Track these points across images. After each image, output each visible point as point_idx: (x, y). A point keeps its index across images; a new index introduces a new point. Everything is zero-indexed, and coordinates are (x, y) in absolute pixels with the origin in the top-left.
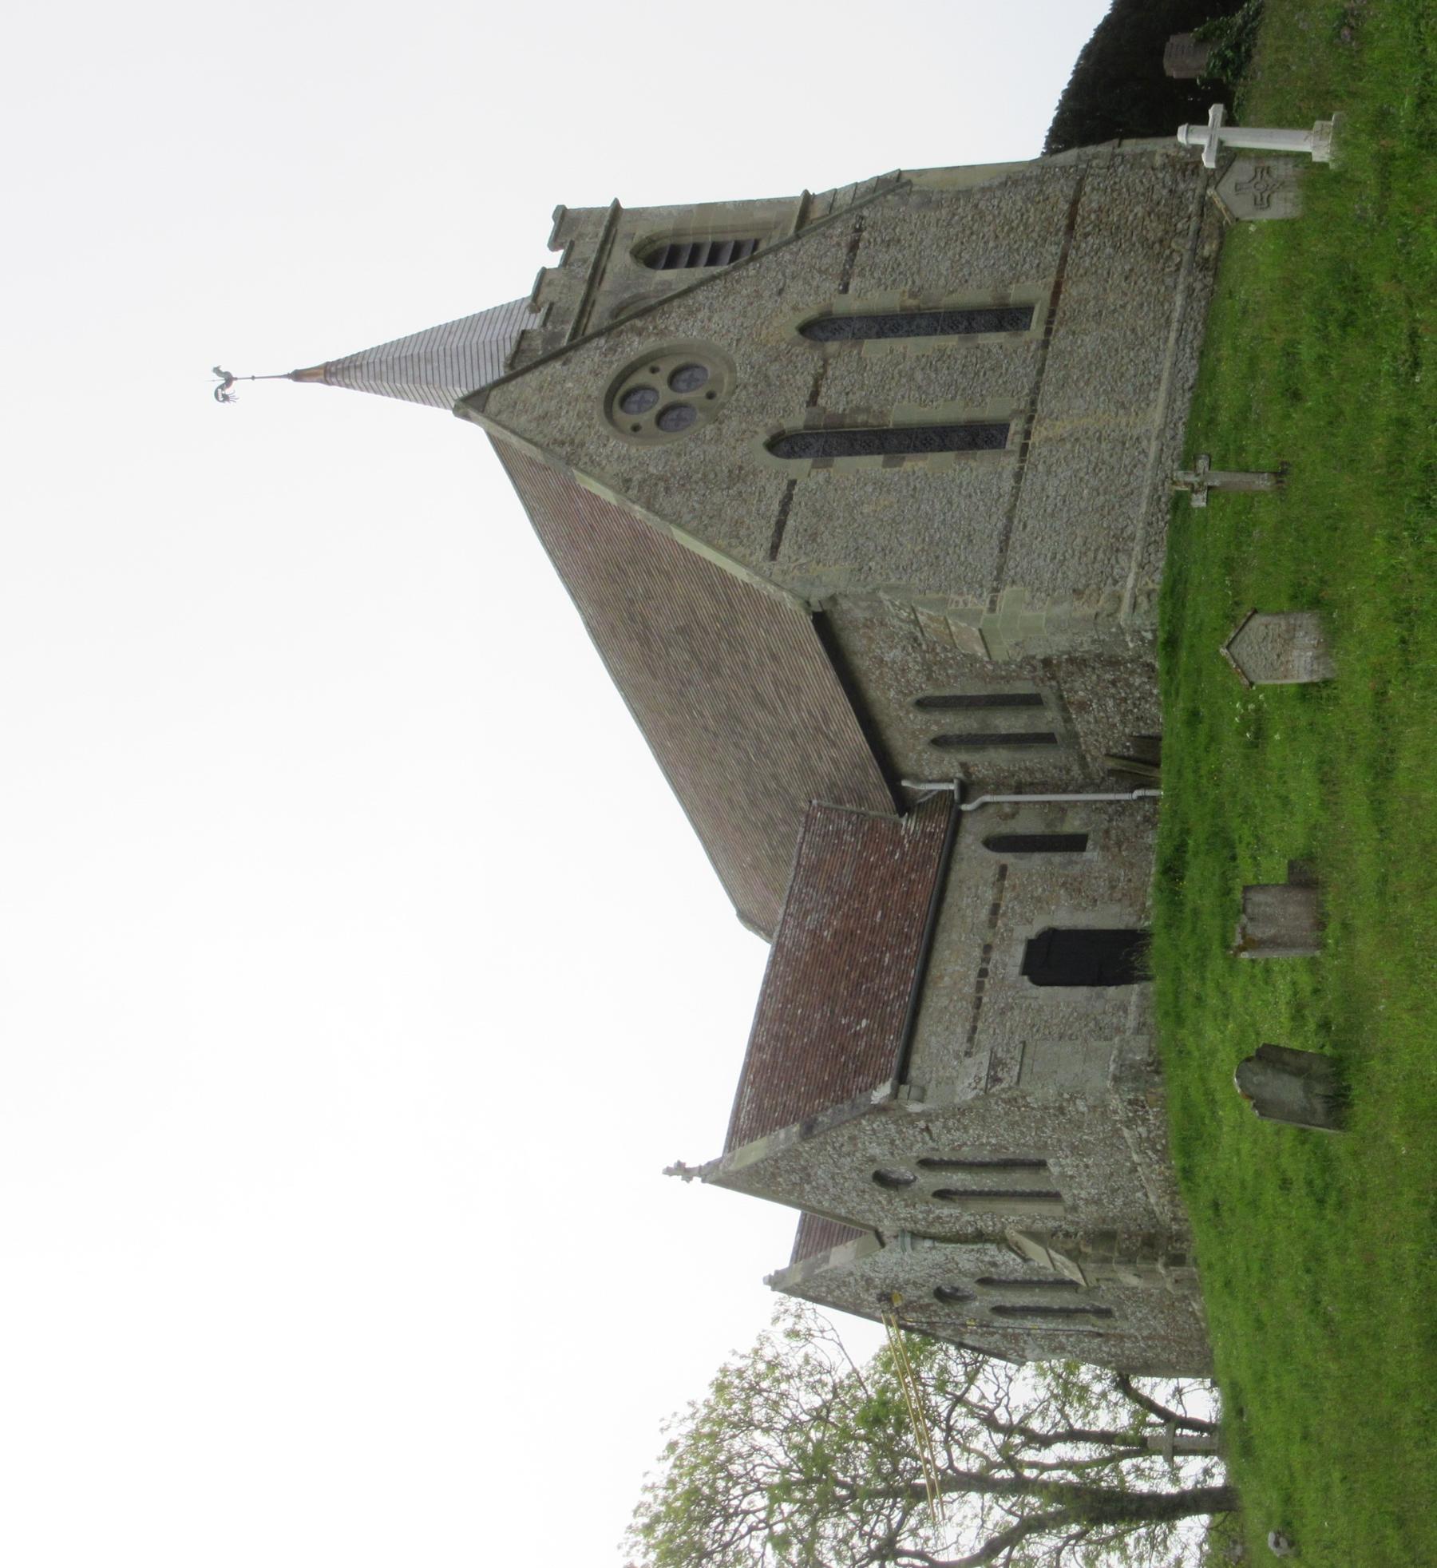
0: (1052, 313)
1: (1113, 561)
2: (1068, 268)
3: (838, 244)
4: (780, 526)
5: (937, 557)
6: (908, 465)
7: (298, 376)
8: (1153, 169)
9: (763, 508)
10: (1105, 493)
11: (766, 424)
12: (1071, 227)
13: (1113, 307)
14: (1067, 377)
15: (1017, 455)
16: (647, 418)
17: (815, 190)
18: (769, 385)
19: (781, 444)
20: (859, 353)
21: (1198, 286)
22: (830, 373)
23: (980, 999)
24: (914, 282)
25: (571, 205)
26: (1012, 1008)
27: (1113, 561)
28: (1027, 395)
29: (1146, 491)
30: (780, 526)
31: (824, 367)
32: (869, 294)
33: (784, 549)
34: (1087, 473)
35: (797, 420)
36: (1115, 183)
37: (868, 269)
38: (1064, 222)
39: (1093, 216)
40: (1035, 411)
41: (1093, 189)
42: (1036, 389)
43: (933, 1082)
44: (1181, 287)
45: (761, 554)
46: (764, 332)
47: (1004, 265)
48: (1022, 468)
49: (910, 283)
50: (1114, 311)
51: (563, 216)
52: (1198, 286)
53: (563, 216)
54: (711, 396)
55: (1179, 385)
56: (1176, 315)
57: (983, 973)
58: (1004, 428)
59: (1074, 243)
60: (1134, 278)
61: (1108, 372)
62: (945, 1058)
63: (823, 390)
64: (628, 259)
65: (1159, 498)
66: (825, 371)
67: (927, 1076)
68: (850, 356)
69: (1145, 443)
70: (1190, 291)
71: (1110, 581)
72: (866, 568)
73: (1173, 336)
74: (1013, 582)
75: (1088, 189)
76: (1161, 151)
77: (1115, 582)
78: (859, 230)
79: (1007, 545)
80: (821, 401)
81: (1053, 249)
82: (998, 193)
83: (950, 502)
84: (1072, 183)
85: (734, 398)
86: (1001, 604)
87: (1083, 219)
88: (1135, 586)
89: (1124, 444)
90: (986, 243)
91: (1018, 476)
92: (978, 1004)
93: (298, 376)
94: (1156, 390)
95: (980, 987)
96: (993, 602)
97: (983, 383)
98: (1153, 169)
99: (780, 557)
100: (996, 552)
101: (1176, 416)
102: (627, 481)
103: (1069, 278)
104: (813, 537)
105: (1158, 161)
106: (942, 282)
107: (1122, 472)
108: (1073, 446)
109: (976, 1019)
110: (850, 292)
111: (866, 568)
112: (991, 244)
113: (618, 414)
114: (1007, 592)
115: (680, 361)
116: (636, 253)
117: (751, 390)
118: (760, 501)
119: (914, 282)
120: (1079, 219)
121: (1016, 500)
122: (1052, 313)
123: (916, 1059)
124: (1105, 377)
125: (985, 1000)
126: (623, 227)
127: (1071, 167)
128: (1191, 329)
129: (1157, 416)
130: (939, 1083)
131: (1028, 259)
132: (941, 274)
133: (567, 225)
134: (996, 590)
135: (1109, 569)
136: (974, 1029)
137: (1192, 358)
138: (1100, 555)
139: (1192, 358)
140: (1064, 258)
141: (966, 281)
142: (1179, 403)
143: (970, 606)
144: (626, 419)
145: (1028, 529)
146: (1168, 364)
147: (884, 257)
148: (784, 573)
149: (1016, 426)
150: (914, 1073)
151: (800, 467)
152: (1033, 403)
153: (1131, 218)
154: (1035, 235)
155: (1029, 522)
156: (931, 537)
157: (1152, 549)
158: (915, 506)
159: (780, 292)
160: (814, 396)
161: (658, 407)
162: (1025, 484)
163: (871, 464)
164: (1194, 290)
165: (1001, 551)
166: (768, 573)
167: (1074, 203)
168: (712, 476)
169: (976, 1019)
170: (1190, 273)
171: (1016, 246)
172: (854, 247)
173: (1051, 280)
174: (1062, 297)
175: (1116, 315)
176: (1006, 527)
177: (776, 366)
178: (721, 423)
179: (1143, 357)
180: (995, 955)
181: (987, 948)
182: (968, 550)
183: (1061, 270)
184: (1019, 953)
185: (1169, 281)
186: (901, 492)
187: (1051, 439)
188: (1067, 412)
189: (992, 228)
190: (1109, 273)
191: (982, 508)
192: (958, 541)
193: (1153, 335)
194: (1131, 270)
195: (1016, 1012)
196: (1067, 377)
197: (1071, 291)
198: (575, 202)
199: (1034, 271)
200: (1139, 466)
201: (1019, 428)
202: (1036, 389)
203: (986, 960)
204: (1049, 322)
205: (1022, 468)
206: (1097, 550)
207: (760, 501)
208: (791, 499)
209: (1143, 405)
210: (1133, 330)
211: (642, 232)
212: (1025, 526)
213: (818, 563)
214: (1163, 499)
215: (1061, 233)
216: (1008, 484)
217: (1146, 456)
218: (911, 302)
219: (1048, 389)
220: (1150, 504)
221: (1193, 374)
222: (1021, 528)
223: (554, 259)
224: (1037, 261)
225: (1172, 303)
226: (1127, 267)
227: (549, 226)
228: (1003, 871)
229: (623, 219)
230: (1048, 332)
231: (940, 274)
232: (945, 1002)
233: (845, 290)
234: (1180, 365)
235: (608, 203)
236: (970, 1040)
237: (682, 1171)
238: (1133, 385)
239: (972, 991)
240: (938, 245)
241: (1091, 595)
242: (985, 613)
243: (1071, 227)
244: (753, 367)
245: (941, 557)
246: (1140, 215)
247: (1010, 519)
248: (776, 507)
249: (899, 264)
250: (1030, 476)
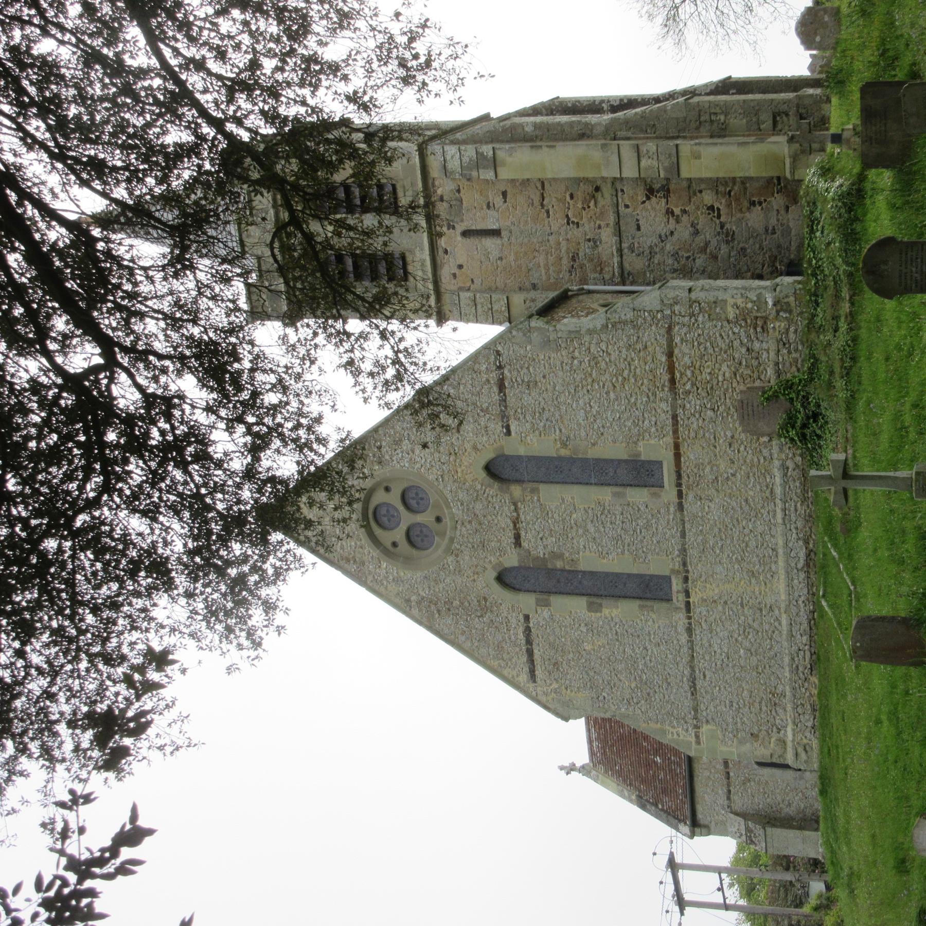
0: (679, 476)
1: (773, 712)
2: (681, 429)
3: (488, 381)
4: (530, 653)
5: (649, 694)
6: (606, 612)
8: (728, 321)
9: (513, 637)
10: (757, 654)
11: (490, 561)
12: (673, 381)
13: (726, 476)
14: (705, 542)
15: (684, 611)
16: (398, 534)
18: (480, 524)
20: (539, 500)
21: (790, 464)
22: (522, 517)
23: (728, 773)
24: (561, 431)
26: (749, 781)
27: (773, 712)
28: (678, 556)
29: (787, 660)
30: (530, 653)
31: (516, 510)
32: (528, 438)
34: (739, 635)
35: (512, 559)
36: (699, 335)
37: (519, 410)
38: (666, 377)
39: (689, 373)
40: (687, 571)
41: (682, 340)
42: (683, 551)
43: (713, 823)
44: (777, 463)
45: (524, 677)
46: (459, 470)
47: (628, 419)
48: (690, 624)
49: (558, 431)
50: (728, 479)
52: (790, 464)
54: (438, 519)
55: (793, 565)
56: (778, 490)
58: (668, 579)
59: (679, 402)
60: (736, 446)
61: (735, 542)
62: (717, 808)
63: (523, 534)
65: (797, 667)
66: (518, 515)
67: (709, 818)
68: (533, 502)
69: (777, 612)
70: (785, 468)
71: (775, 729)
72: (601, 698)
73: (779, 515)
74: (707, 722)
75: (677, 340)
76: (731, 301)
77: (779, 730)
78: (500, 367)
79: (695, 689)
80: (525, 544)
81: (664, 405)
82: (603, 336)
83: (645, 648)
84: (663, 331)
85: (458, 533)
86: (703, 738)
87: (681, 374)
88: (793, 741)
89: (761, 610)
90: (608, 393)
91: (689, 630)
92: (728, 777)
94: (776, 562)
96: (697, 737)
97: (642, 541)
98: (728, 321)
99: (538, 680)
100: (689, 694)
101: (796, 594)
102: (408, 601)
103: (684, 440)
105: (731, 313)
106: (583, 434)
107: (766, 637)
108: (724, 609)
109: (729, 785)
110: (513, 433)
111: (601, 698)
112: (612, 395)
113: (378, 531)
114: (705, 729)
115: (405, 485)
117: (468, 526)
118: (508, 630)
119: (561, 431)
120: (678, 375)
121: (693, 652)
122: (679, 476)
123: (699, 808)
124: (734, 546)
125: (732, 774)
127: (658, 312)
128: (792, 509)
129: (781, 585)
130: (716, 824)
131: (646, 416)
132: (580, 424)
134: (696, 727)
135: (772, 720)
137: (799, 539)
138: (764, 708)
139: (799, 539)
140: (675, 417)
141: (602, 434)
142: (796, 581)
143: (682, 737)
144: (386, 537)
145: (707, 679)
146: (781, 542)
147: (527, 400)
148: (546, 694)
149: (676, 585)
150: (700, 816)
151: (527, 601)
152: (685, 564)
153: (720, 379)
154: (644, 388)
155: (707, 673)
156: (640, 677)
157: (800, 710)
158: (621, 648)
160: (517, 537)
161: (401, 508)
162: (697, 638)
163: (577, 605)
164: (788, 468)
165: (693, 694)
166: (534, 693)
167: (670, 355)
168: (466, 604)
169: (729, 785)
170: (781, 450)
171: (633, 400)
172: (501, 386)
173: (669, 439)
174: (682, 459)
175: (730, 483)
176: (691, 674)
177: (479, 506)
178: (457, 556)
179: (760, 529)
182: (669, 691)
183: (675, 432)
185: (766, 452)
186: (607, 635)
187: (706, 600)
188: (712, 576)
189: (607, 376)
190: (715, 438)
191: (670, 656)
192: (660, 683)
193: (763, 507)
194: (732, 437)
195: (752, 783)
196: (705, 542)
197: (690, 455)
199: (653, 429)
200: (776, 632)
201: (680, 588)
202: (683, 551)
204: (679, 485)
205: (690, 624)
206: (760, 703)
207: (508, 630)
208: (530, 631)
209: (769, 576)
210: (746, 501)
212: (705, 676)
213: (566, 689)
214: (801, 669)
215: (666, 389)
216: (684, 638)
217: (780, 624)
218: (564, 452)
219: (693, 553)
220: (791, 672)
221: (802, 554)
222: (702, 677)
224: (654, 419)
225: (772, 477)
226: (729, 434)
230: (680, 494)
231: (579, 425)
232: (707, 773)
233: (509, 433)
234: (790, 545)
236: (729, 798)
237: (570, 769)
238: (758, 556)
239: (722, 767)
240: (569, 393)
241: (764, 739)
242: (693, 743)
243: (673, 381)
244: (462, 504)
245: (652, 694)
246: (727, 375)
247: (693, 669)
248: (521, 636)
249: (544, 409)
250: (698, 632)
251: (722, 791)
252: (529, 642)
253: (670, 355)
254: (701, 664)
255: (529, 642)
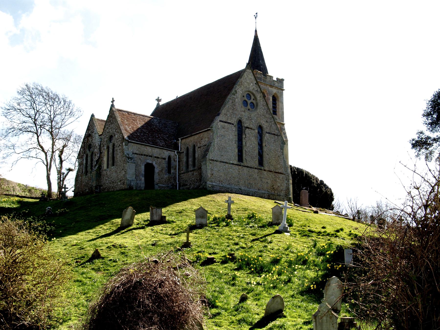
3: (275, 132)
7: (256, 31)
12: (276, 173)
17: (285, 126)
19: (240, 122)
25: (284, 82)
30: (226, 122)
33: (222, 123)
38: (277, 171)
51: (283, 80)
53: (283, 80)
57: (147, 156)
64: (274, 92)
78: (277, 135)
91: (233, 164)
92: (142, 155)
93: (256, 31)
95: (145, 155)
99: (220, 122)
104: (224, 128)
109: (139, 154)
116: (275, 94)
126: (280, 91)
133: (281, 81)
136: (137, 154)
159: (267, 122)
167: (280, 173)
169: (139, 154)
172: (274, 134)
180: (150, 158)
181: (151, 156)
184: (150, 162)
185: (266, 190)
198: (285, 82)
203: (149, 156)
211: (279, 95)
216: (231, 162)
223: (275, 79)
227: (280, 78)
228: (165, 159)
229: (281, 91)
235: (284, 89)
237: (113, 101)
243: (276, 173)
248: (229, 121)
251: (137, 152)
252: (228, 123)
253: (280, 173)
254: (227, 165)
255: (228, 123)
